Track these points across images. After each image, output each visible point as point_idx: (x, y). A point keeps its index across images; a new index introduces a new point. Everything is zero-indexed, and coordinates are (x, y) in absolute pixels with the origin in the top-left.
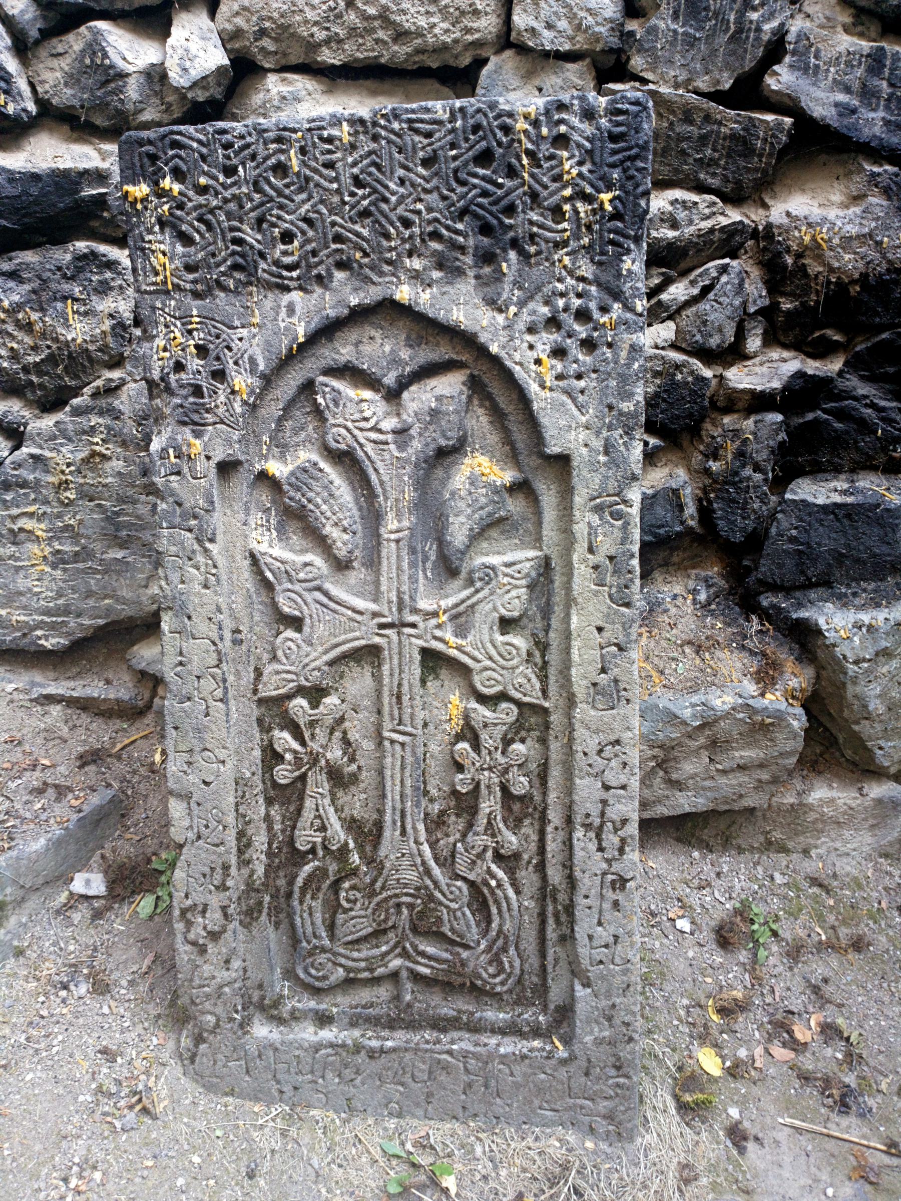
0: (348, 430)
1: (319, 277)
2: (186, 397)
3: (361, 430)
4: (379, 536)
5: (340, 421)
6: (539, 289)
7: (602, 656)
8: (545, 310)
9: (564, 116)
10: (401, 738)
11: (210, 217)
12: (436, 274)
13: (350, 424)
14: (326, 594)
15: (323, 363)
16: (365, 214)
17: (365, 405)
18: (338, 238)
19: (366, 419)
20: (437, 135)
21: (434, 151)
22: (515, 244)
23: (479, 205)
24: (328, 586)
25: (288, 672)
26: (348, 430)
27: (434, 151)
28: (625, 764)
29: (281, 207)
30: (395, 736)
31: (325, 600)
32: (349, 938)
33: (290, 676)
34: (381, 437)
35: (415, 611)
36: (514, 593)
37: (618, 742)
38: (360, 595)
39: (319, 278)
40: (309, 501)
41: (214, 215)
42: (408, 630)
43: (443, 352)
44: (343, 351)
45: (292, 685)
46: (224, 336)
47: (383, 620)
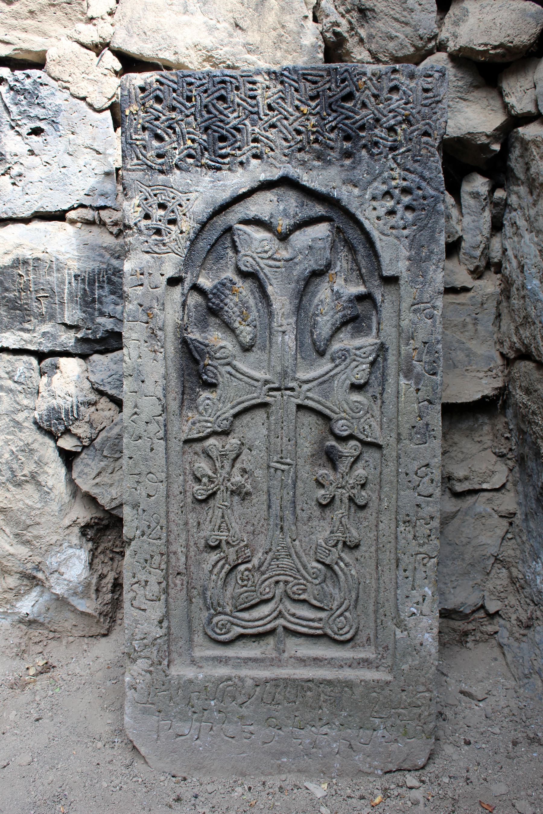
0: (254, 259)
1: (241, 163)
2: (150, 236)
3: (262, 258)
4: (270, 328)
5: (249, 253)
6: (380, 174)
7: (419, 408)
8: (384, 188)
9: (397, 76)
10: (283, 467)
11: (175, 125)
12: (316, 163)
13: (255, 255)
14: (234, 368)
15: (240, 216)
16: (273, 126)
17: (265, 243)
18: (255, 140)
19: (266, 252)
20: (319, 84)
21: (318, 92)
22: (365, 146)
23: (346, 125)
24: (235, 363)
25: (207, 421)
26: (254, 259)
27: (318, 92)
28: (432, 481)
29: (222, 121)
30: (278, 465)
31: (233, 372)
32: (243, 606)
33: (209, 425)
34: (278, 264)
35: (294, 379)
36: (360, 368)
37: (427, 465)
38: (255, 368)
39: (241, 163)
40: (226, 305)
41: (178, 124)
42: (288, 392)
43: (319, 210)
44: (253, 209)
45: (209, 430)
46: (177, 198)
47: (272, 386)
